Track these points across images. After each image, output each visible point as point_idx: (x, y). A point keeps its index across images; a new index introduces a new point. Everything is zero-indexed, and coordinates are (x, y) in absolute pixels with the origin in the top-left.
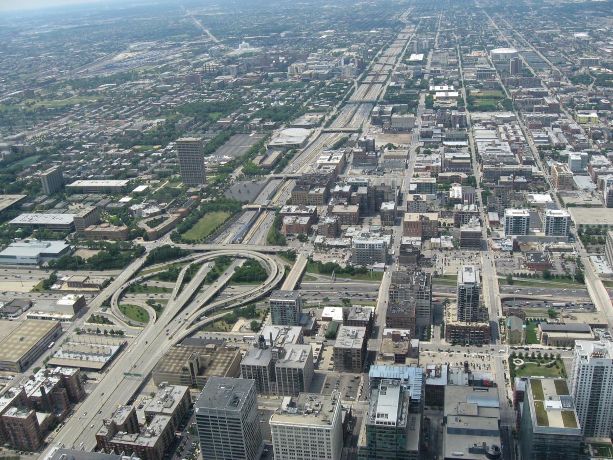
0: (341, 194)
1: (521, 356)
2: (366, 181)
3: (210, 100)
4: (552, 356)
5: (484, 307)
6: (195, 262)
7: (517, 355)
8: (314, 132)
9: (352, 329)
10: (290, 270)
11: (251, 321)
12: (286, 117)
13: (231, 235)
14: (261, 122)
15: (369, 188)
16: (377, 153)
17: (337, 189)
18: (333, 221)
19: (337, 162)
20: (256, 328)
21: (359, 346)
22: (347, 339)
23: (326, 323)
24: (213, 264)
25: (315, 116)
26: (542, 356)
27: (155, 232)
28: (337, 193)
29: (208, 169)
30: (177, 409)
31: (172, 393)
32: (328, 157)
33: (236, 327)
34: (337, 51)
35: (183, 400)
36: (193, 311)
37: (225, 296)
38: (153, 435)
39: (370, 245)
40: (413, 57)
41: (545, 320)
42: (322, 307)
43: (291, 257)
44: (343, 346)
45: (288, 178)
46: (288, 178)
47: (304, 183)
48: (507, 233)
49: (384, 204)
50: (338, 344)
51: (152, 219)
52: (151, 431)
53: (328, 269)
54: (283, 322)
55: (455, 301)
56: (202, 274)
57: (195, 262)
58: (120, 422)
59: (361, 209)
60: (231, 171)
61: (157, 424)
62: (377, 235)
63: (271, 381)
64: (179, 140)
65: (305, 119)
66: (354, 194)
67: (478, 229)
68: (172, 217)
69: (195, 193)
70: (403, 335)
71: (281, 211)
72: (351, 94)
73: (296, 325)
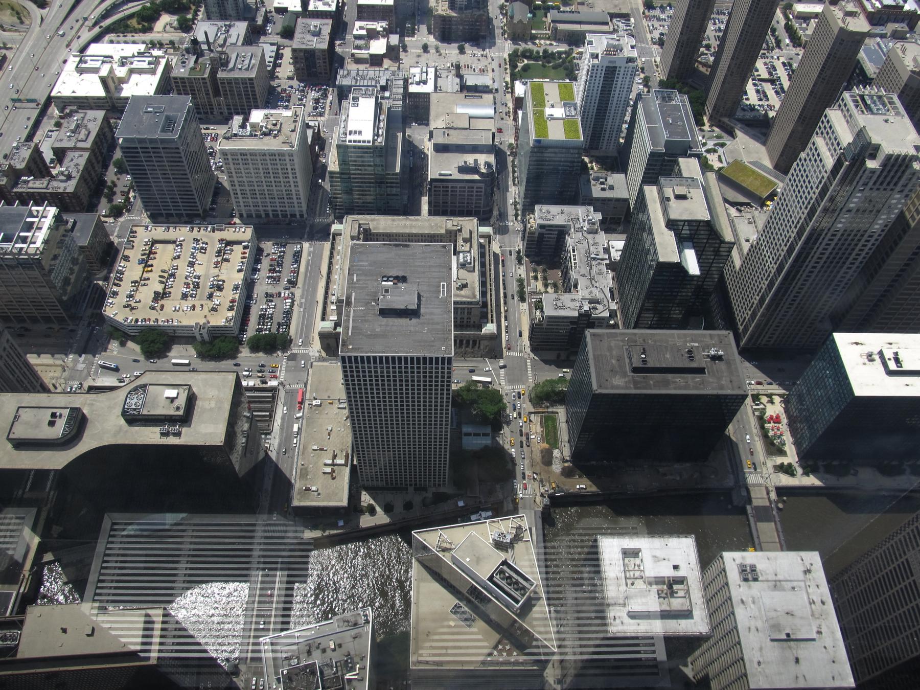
9: (314, 23)
20: (186, 26)
21: (325, 46)
22: (309, 37)
30: (95, 142)
31: (85, 122)
33: (159, 25)
35: (101, 128)
38: (69, 177)
44: (304, 47)
50: (296, 43)
52: (66, 173)
54: (223, 16)
58: (20, 166)
61: (72, 164)
63: (215, 96)
70: (379, 29)
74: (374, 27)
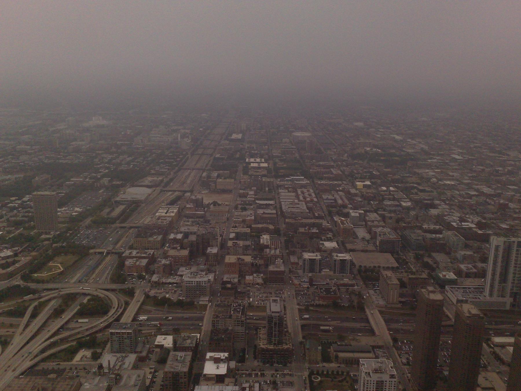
0: (175, 239)
1: (318, 374)
2: (196, 230)
3: (66, 161)
4: (343, 372)
5: (287, 331)
6: (41, 300)
7: (315, 373)
8: (155, 190)
9: (180, 354)
10: (129, 304)
11: (92, 350)
12: (132, 178)
13: (78, 275)
14: (110, 181)
15: (198, 236)
16: (204, 209)
17: (172, 236)
18: (168, 263)
19: (173, 214)
20: (96, 357)
21: (186, 369)
22: (176, 364)
23: (158, 350)
24: (60, 301)
25: (155, 178)
26: (335, 373)
27: (7, 273)
28: (172, 239)
29: (63, 220)
32: (165, 211)
33: (78, 357)
34: (176, 128)
36: (36, 346)
37: (68, 329)
39: (197, 282)
40: (234, 136)
41: (336, 342)
42: (156, 336)
43: (130, 293)
44: (172, 370)
45: (131, 228)
46: (131, 228)
47: (144, 232)
48: (304, 272)
49: (209, 248)
51: (4, 261)
53: (162, 303)
55: (265, 327)
56: (49, 310)
57: (41, 300)
59: (191, 252)
60: (81, 221)
62: (204, 273)
64: (35, 193)
65: (148, 180)
66: (186, 240)
67: (282, 268)
68: (24, 260)
69: (48, 239)
71: (124, 255)
72: (185, 162)
73: (132, 352)
74: (219, 356)
